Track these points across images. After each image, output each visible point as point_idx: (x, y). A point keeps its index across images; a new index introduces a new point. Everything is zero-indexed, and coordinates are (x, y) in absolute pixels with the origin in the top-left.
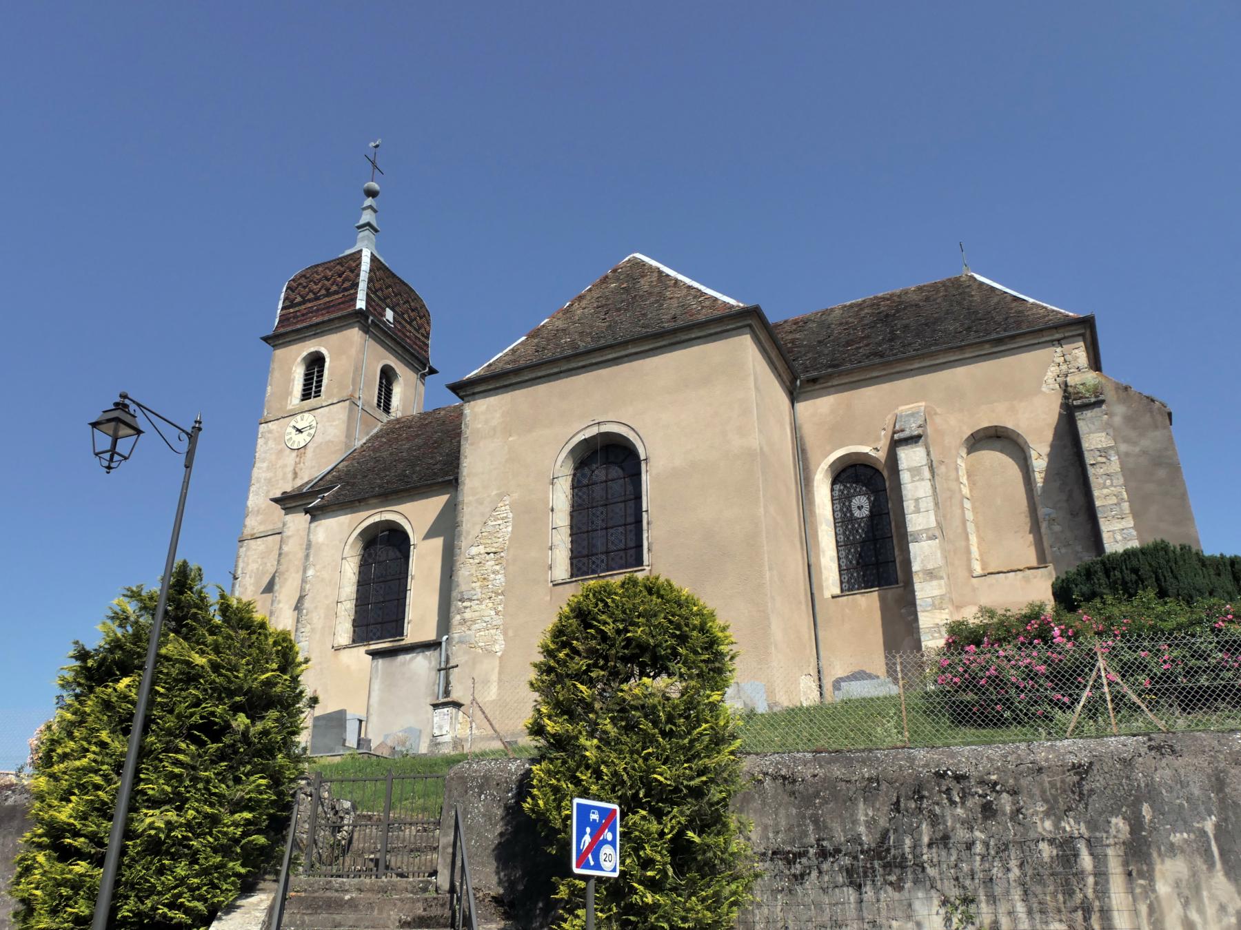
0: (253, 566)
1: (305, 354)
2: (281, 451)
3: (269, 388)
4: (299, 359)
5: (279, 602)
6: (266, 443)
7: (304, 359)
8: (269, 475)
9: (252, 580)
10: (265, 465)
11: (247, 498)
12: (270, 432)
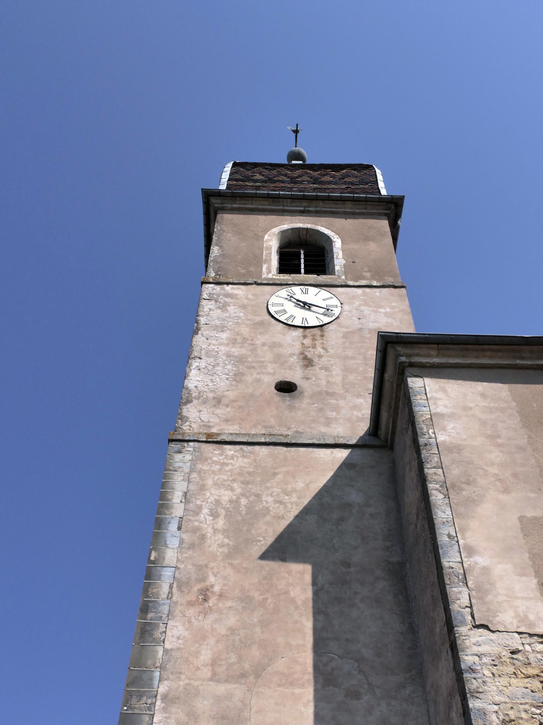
0: (218, 494)
1: (285, 227)
4: (276, 230)
5: (471, 551)
6: (224, 307)
7: (283, 232)
9: (221, 523)
10: (224, 335)
11: (185, 376)
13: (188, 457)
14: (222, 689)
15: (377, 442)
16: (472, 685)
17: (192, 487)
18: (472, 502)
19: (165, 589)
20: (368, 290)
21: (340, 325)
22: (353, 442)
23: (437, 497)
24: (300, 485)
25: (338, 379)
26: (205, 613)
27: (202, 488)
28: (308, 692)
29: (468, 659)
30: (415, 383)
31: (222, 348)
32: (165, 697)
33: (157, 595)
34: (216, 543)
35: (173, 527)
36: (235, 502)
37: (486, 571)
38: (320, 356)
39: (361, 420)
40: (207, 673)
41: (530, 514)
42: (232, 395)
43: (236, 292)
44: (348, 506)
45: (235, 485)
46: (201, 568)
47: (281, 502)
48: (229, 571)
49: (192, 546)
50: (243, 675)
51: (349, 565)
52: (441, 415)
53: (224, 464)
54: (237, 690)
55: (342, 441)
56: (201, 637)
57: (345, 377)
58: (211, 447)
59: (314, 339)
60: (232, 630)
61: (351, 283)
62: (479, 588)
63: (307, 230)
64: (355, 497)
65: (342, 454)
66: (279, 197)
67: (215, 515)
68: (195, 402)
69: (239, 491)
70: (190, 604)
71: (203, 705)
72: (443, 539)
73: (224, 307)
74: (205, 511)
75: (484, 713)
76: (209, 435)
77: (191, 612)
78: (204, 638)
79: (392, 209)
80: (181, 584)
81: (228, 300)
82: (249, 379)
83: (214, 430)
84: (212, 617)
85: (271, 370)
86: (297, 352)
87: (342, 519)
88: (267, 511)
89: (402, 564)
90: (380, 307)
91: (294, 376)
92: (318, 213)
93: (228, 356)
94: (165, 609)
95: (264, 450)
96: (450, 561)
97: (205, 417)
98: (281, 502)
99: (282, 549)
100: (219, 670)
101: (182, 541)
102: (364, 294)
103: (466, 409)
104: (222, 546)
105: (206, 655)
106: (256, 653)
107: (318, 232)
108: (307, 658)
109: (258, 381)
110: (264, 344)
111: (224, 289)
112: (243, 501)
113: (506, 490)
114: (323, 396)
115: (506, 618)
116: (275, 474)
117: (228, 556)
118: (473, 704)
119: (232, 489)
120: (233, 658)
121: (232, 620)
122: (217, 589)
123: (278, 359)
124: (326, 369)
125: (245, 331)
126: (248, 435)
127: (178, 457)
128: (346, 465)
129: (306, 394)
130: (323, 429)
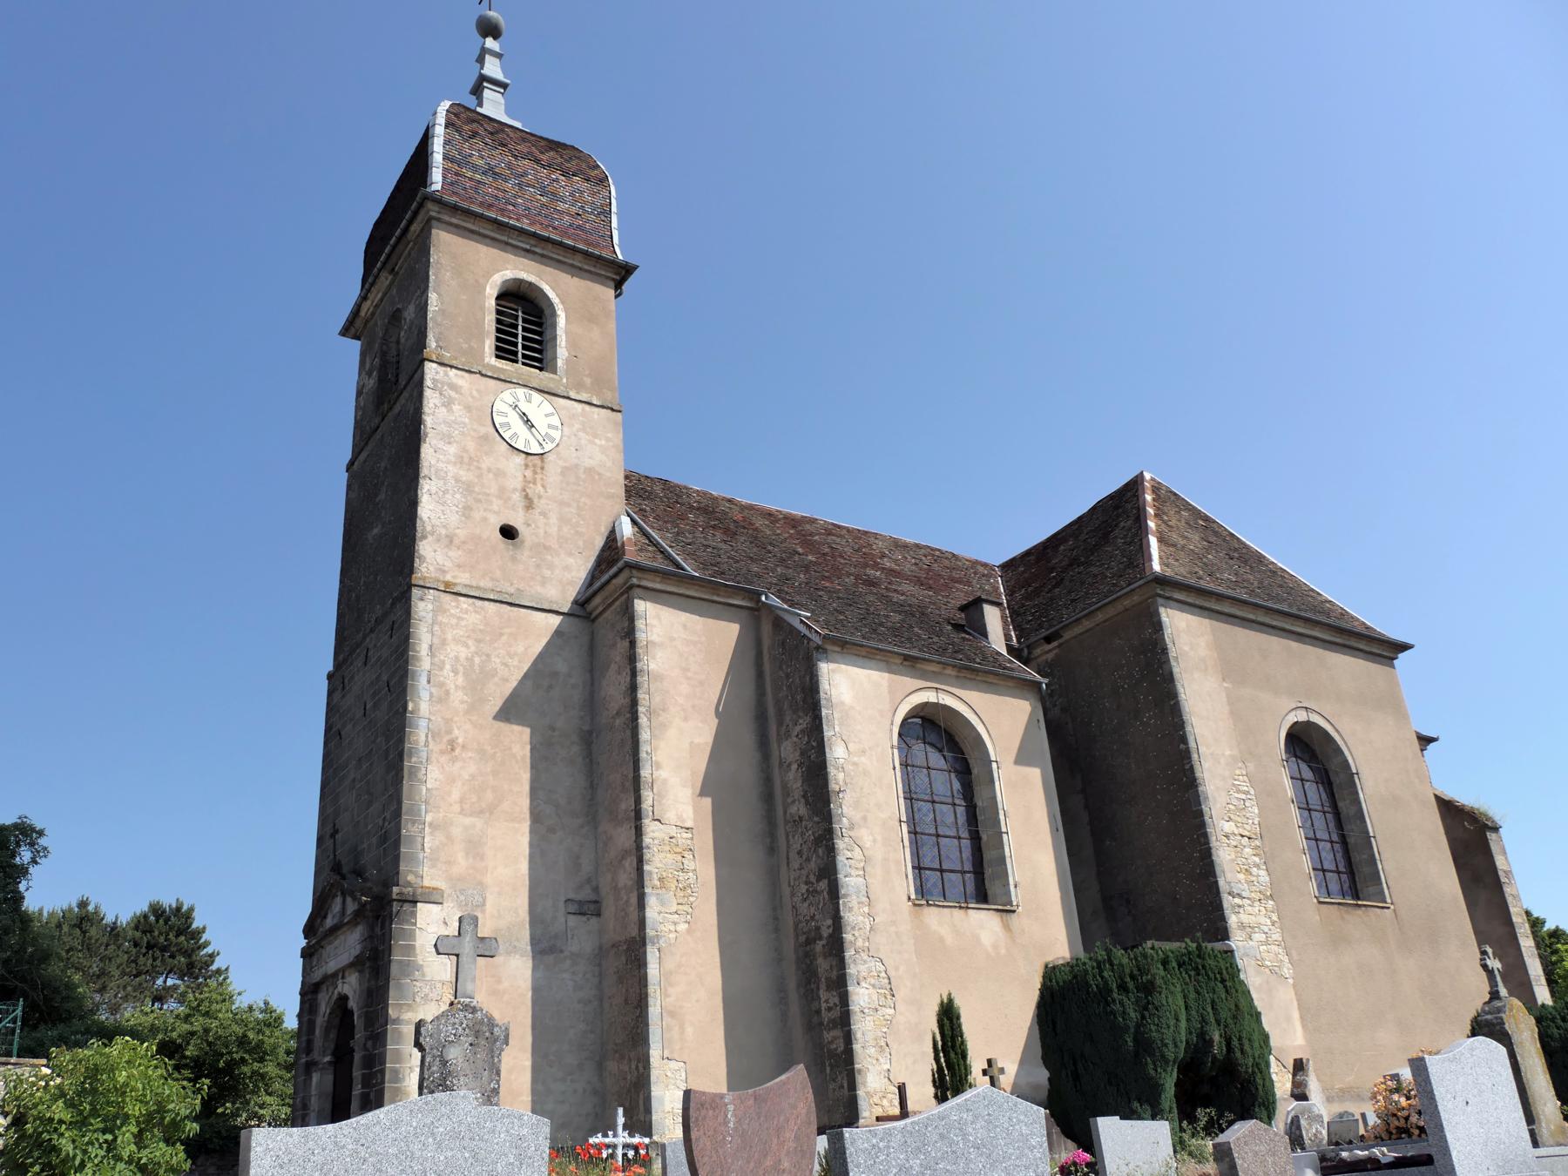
0: (457, 651)
2: (485, 438)
3: (433, 297)
5: (659, 767)
6: (448, 404)
8: (465, 475)
9: (460, 680)
10: (452, 449)
12: (453, 387)
13: (430, 607)
14: (468, 821)
15: (581, 613)
16: (647, 856)
17: (436, 641)
18: (664, 727)
19: (423, 738)
20: (587, 407)
21: (558, 454)
22: (565, 610)
23: (643, 720)
24: (520, 649)
25: (554, 530)
26: (454, 760)
27: (444, 642)
28: (525, 827)
29: (647, 840)
30: (640, 606)
31: (450, 467)
32: (431, 824)
33: (417, 742)
34: (458, 698)
35: (423, 680)
36: (470, 660)
37: (665, 781)
38: (540, 497)
39: (571, 583)
40: (457, 808)
41: (697, 741)
42: (462, 534)
43: (460, 382)
44: (555, 674)
45: (470, 643)
46: (448, 721)
47: (506, 665)
48: (468, 726)
49: (440, 700)
50: (482, 812)
51: (553, 729)
52: (654, 643)
53: (460, 618)
54: (478, 823)
55: (555, 608)
56: (452, 780)
57: (560, 529)
58: (448, 597)
59: (535, 473)
60: (473, 777)
61: (572, 394)
62: (659, 794)
63: (531, 284)
64: (561, 667)
65: (556, 621)
66: (506, 225)
67: (456, 672)
68: (430, 538)
69: (473, 649)
70: (442, 752)
71: (456, 831)
72: (643, 755)
73: (448, 404)
74: (448, 667)
75: (650, 873)
76: (447, 584)
77: (444, 759)
78: (454, 781)
79: (619, 274)
80: (434, 734)
81: (453, 394)
82: (477, 515)
83: (448, 578)
84: (458, 764)
85: (495, 508)
86: (519, 487)
87: (550, 687)
88: (494, 673)
89: (590, 733)
90: (596, 436)
91: (517, 521)
92: (544, 259)
93: (457, 481)
94: (424, 755)
95: (492, 606)
96: (645, 773)
97: (440, 559)
98: (506, 665)
99: (510, 711)
100: (466, 807)
101: (431, 695)
102: (583, 413)
103: (672, 639)
104: (462, 702)
105: (456, 795)
106: (489, 796)
107: (542, 291)
108: (525, 803)
109: (485, 519)
110: (489, 470)
111: (446, 374)
112: (477, 660)
113: (686, 719)
114: (542, 548)
115: (670, 816)
116: (501, 634)
117: (467, 712)
118: (646, 868)
119: (467, 646)
120: (474, 799)
121: (472, 768)
122: (460, 741)
123: (502, 493)
124: (543, 514)
125: (471, 445)
126: (478, 588)
127: (421, 605)
128: (558, 633)
129: (527, 544)
130: (539, 589)
